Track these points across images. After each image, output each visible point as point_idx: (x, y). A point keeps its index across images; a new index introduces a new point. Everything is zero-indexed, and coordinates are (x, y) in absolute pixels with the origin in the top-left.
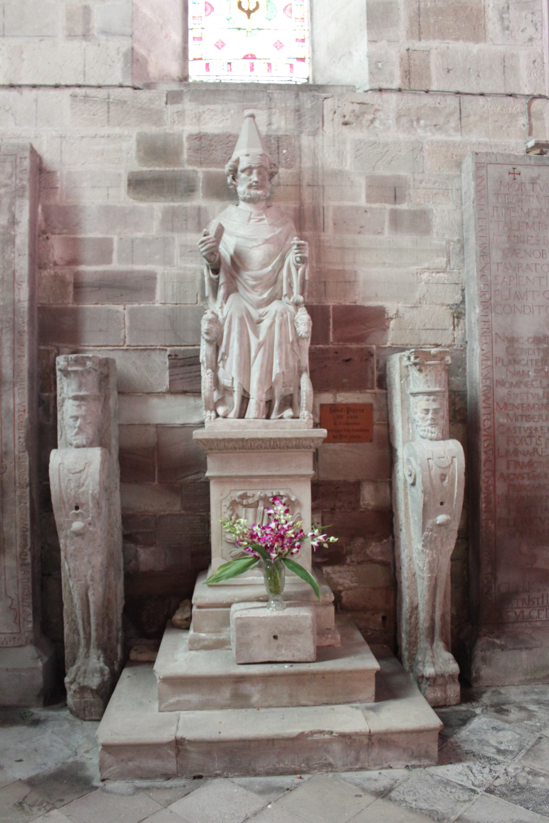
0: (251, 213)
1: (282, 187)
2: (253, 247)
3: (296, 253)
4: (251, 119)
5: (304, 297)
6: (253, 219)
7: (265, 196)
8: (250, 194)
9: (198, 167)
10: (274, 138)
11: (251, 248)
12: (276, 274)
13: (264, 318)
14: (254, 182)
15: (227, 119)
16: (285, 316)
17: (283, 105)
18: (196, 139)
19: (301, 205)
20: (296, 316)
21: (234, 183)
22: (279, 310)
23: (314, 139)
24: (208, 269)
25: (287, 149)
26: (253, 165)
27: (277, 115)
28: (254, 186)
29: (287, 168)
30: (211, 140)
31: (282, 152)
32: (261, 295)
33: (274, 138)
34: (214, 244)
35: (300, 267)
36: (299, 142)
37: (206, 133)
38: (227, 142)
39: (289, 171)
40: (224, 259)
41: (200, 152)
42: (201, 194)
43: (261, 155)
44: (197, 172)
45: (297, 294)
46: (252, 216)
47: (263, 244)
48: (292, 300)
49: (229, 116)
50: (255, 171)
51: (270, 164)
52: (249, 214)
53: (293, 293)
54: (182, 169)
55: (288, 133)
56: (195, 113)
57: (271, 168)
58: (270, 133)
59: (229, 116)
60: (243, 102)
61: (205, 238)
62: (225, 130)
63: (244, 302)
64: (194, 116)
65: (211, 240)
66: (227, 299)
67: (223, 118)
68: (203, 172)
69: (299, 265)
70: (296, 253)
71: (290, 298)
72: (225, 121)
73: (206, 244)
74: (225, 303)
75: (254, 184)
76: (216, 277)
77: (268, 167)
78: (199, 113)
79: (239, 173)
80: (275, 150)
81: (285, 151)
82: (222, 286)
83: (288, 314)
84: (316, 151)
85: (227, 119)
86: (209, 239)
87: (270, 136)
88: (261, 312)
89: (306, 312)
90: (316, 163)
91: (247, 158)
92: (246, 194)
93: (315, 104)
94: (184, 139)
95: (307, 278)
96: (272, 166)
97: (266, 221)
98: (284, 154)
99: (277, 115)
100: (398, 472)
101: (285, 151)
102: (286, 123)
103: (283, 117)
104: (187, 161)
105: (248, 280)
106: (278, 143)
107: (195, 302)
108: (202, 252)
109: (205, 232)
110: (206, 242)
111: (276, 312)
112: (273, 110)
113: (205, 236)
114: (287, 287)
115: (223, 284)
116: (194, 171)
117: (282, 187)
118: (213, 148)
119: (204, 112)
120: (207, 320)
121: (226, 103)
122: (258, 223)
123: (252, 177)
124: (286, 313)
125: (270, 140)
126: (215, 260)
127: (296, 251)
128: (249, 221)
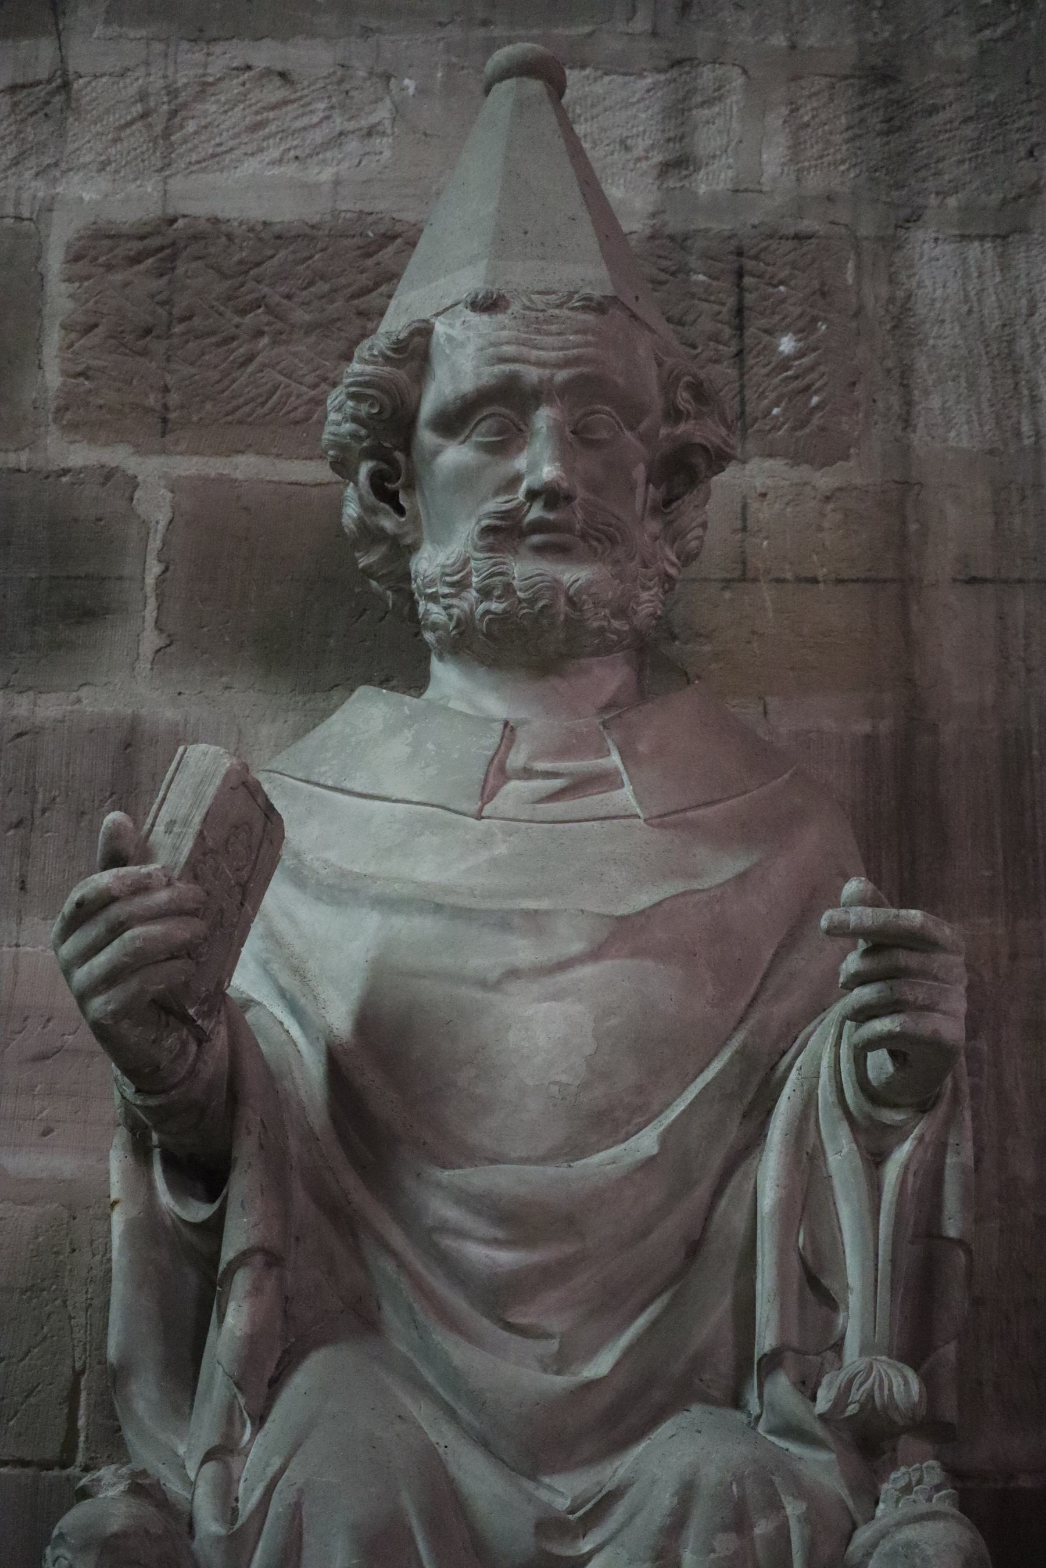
0: (509, 728)
1: (767, 593)
2: (513, 973)
3: (863, 1014)
4: (535, 86)
5: (928, 1380)
6: (527, 773)
7: (621, 612)
8: (508, 590)
9: (140, 450)
10: (706, 256)
11: (496, 987)
12: (702, 1192)
13: (586, 1546)
14: (532, 495)
15: (370, 132)
16: (762, 1528)
17: (779, 40)
18: (135, 260)
20: (863, 1535)
21: (388, 523)
22: (710, 1476)
23: (1005, 265)
24: (140, 1150)
25: (804, 329)
26: (532, 374)
27: (735, 100)
28: (539, 526)
29: (796, 458)
30: (245, 267)
31: (772, 349)
32: (561, 1363)
33: (706, 256)
34: (180, 931)
35: (899, 1133)
36: (892, 280)
37: (216, 221)
38: (364, 280)
39: (825, 480)
40: (270, 1078)
41: (159, 347)
42: (150, 640)
43: (599, 307)
44: (133, 483)
45: (865, 1349)
46: (517, 759)
47: (595, 954)
48: (823, 1403)
49: (382, 113)
50: (544, 418)
51: (669, 384)
52: (492, 739)
53: (838, 1347)
54: (23, 459)
55: (807, 225)
56: (143, 96)
57: (674, 415)
58: (675, 224)
59: (382, 113)
60: (485, 23)
61: (105, 879)
62: (348, 205)
63: (420, 1411)
64: (139, 108)
65: (161, 897)
66: (276, 1384)
67: (339, 122)
68: (174, 486)
69: (891, 1117)
70: (863, 1014)
71: (808, 1388)
72: (353, 145)
73: (116, 930)
74: (260, 1420)
75: (535, 512)
76: (200, 1212)
77: (654, 397)
78: (172, 92)
79: (426, 437)
80: (715, 338)
81: (787, 344)
82: (242, 1281)
83: (793, 1509)
84: (1024, 344)
85: (370, 132)
86: (141, 888)
87: (681, 241)
88: (562, 1504)
89: (943, 1501)
90: (1026, 428)
91: (482, 321)
92: (472, 594)
93: (1008, 36)
94: (55, 261)
95: (952, 1229)
96: (683, 398)
97: (625, 796)
98: (785, 363)
99: (735, 100)
101: (787, 344)
102: (796, 148)
103: (775, 120)
104: (61, 410)
105: (461, 1234)
106: (740, 288)
107: (52, 1450)
108: (83, 998)
109: (115, 834)
110: (116, 911)
111: (687, 1493)
112: (707, 75)
113: (114, 859)
114: (782, 1291)
115: (242, 1259)
116: (108, 475)
117: (767, 593)
118: (259, 316)
119: (204, 89)
120: (84, 1547)
121: (366, 32)
122: (558, 808)
123: (521, 463)
124: (775, 1505)
125: (682, 270)
126: (193, 1072)
127: (864, 994)
128: (487, 794)
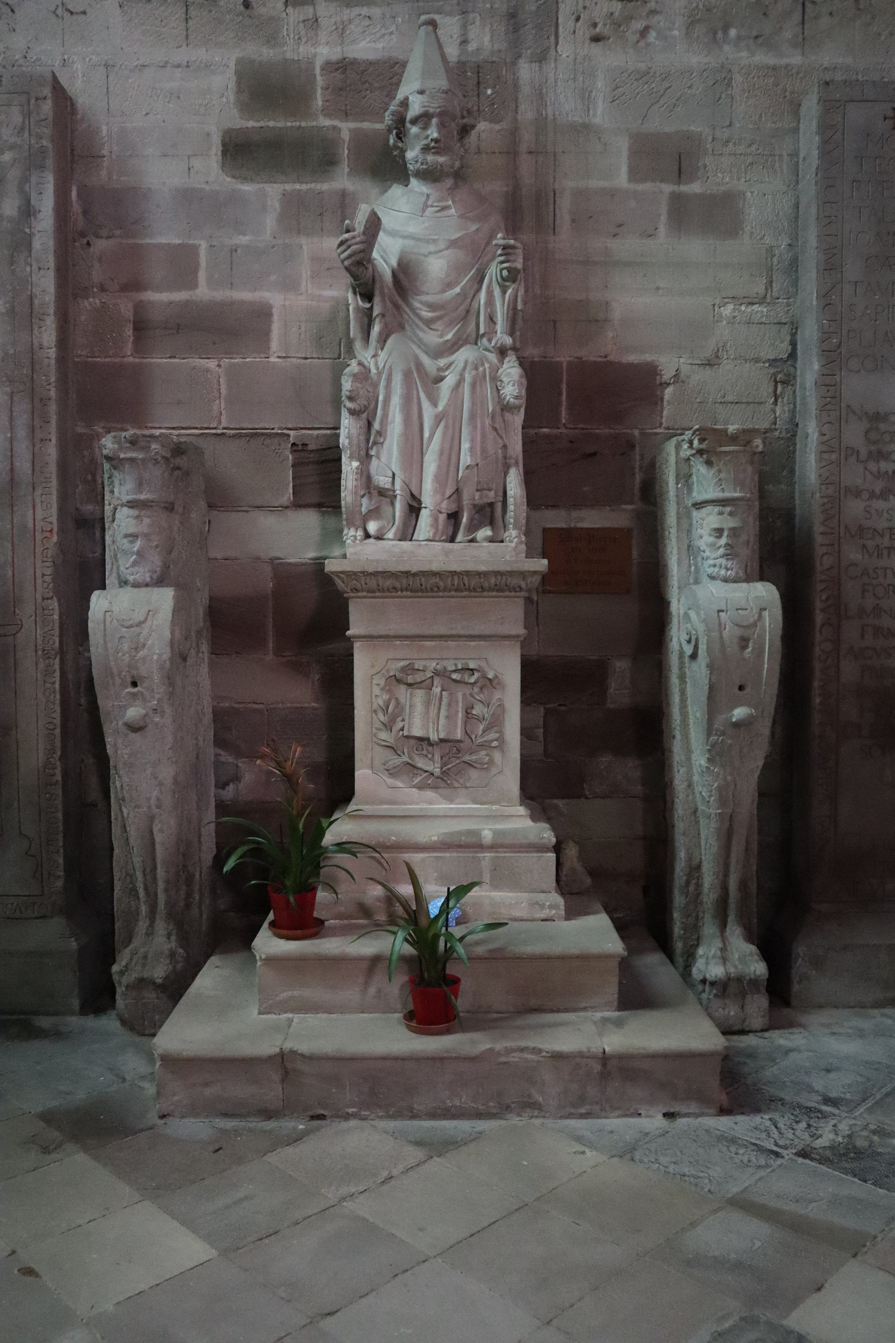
0: (428, 195)
2: (430, 253)
3: (502, 262)
4: (430, 28)
5: (514, 340)
6: (432, 206)
7: (452, 167)
8: (427, 163)
9: (341, 121)
12: (469, 300)
13: (447, 373)
14: (432, 140)
15: (391, 33)
16: (481, 369)
17: (488, 6)
18: (337, 70)
19: (517, 187)
20: (500, 371)
21: (400, 145)
22: (471, 359)
23: (541, 67)
24: (355, 293)
26: (431, 110)
28: (433, 148)
29: (491, 121)
30: (363, 72)
32: (441, 336)
35: (508, 287)
37: (355, 59)
38: (391, 75)
39: (497, 127)
40: (380, 276)
42: (347, 170)
43: (446, 92)
44: (340, 130)
45: (501, 333)
46: (430, 203)
48: (493, 344)
49: (393, 28)
50: (434, 121)
52: (424, 199)
53: (496, 332)
54: (314, 123)
55: (494, 59)
56: (335, 23)
57: (463, 117)
58: (463, 59)
61: (346, 236)
62: (386, 54)
63: (414, 347)
64: (334, 27)
65: (358, 239)
66: (385, 341)
69: (507, 284)
70: (502, 262)
71: (490, 341)
72: (387, 37)
73: (349, 247)
74: (382, 349)
75: (433, 144)
76: (368, 305)
77: (459, 114)
78: (343, 22)
79: (408, 125)
81: (489, 92)
82: (377, 320)
83: (487, 365)
84: (544, 91)
85: (391, 33)
86: (354, 237)
88: (442, 365)
89: (516, 364)
90: (544, 113)
91: (419, 96)
92: (419, 164)
94: (318, 71)
95: (519, 307)
96: (465, 113)
97: (453, 211)
98: (489, 96)
100: (671, 640)
103: (487, 29)
104: (323, 110)
105: (421, 309)
107: (336, 356)
108: (343, 261)
109: (347, 226)
110: (349, 243)
111: (466, 362)
112: (471, 16)
113: (348, 231)
114: (485, 320)
116: (334, 128)
117: (484, 156)
118: (367, 85)
119: (350, 21)
122: (439, 214)
123: (429, 132)
124: (483, 365)
127: (502, 258)
128: (424, 211)
